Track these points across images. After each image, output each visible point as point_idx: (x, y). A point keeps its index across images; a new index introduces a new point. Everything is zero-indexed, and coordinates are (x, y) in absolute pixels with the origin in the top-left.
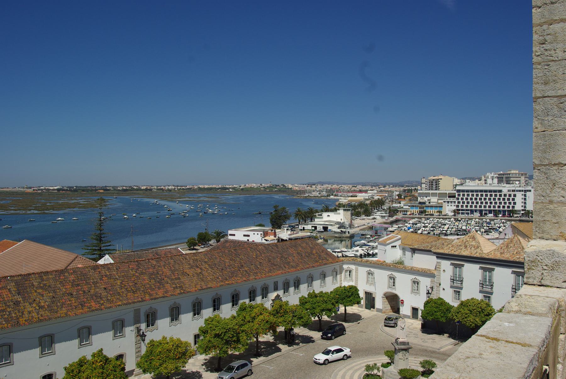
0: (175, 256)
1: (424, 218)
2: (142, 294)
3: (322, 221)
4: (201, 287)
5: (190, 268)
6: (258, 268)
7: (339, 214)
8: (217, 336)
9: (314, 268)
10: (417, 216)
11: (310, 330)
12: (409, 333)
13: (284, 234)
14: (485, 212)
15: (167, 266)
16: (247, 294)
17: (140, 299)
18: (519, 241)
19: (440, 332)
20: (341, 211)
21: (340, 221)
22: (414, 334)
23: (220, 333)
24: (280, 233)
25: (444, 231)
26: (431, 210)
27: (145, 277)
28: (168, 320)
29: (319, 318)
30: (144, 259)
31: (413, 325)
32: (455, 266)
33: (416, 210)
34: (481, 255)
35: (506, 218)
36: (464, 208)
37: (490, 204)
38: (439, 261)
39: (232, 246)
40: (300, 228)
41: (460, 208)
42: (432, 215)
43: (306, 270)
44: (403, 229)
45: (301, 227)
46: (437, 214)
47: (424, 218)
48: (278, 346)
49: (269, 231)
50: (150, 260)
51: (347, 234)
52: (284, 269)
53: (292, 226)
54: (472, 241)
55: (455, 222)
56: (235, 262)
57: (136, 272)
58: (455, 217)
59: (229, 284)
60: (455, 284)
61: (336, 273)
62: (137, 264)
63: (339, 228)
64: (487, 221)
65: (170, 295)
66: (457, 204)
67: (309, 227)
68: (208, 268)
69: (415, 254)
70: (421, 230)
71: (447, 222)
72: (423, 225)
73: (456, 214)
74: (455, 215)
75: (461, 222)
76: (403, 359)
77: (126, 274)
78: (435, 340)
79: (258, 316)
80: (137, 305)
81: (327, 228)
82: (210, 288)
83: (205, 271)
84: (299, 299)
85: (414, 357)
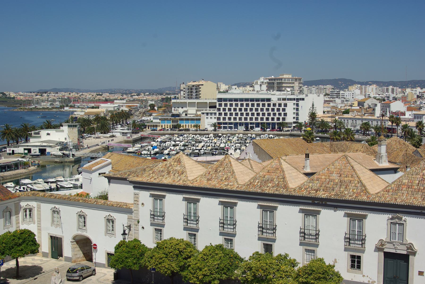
10: (169, 132)
31: (106, 276)
32: (155, 197)
34: (185, 183)
38: (137, 191)
42: (188, 130)
54: (177, 165)
60: (155, 220)
69: (111, 184)
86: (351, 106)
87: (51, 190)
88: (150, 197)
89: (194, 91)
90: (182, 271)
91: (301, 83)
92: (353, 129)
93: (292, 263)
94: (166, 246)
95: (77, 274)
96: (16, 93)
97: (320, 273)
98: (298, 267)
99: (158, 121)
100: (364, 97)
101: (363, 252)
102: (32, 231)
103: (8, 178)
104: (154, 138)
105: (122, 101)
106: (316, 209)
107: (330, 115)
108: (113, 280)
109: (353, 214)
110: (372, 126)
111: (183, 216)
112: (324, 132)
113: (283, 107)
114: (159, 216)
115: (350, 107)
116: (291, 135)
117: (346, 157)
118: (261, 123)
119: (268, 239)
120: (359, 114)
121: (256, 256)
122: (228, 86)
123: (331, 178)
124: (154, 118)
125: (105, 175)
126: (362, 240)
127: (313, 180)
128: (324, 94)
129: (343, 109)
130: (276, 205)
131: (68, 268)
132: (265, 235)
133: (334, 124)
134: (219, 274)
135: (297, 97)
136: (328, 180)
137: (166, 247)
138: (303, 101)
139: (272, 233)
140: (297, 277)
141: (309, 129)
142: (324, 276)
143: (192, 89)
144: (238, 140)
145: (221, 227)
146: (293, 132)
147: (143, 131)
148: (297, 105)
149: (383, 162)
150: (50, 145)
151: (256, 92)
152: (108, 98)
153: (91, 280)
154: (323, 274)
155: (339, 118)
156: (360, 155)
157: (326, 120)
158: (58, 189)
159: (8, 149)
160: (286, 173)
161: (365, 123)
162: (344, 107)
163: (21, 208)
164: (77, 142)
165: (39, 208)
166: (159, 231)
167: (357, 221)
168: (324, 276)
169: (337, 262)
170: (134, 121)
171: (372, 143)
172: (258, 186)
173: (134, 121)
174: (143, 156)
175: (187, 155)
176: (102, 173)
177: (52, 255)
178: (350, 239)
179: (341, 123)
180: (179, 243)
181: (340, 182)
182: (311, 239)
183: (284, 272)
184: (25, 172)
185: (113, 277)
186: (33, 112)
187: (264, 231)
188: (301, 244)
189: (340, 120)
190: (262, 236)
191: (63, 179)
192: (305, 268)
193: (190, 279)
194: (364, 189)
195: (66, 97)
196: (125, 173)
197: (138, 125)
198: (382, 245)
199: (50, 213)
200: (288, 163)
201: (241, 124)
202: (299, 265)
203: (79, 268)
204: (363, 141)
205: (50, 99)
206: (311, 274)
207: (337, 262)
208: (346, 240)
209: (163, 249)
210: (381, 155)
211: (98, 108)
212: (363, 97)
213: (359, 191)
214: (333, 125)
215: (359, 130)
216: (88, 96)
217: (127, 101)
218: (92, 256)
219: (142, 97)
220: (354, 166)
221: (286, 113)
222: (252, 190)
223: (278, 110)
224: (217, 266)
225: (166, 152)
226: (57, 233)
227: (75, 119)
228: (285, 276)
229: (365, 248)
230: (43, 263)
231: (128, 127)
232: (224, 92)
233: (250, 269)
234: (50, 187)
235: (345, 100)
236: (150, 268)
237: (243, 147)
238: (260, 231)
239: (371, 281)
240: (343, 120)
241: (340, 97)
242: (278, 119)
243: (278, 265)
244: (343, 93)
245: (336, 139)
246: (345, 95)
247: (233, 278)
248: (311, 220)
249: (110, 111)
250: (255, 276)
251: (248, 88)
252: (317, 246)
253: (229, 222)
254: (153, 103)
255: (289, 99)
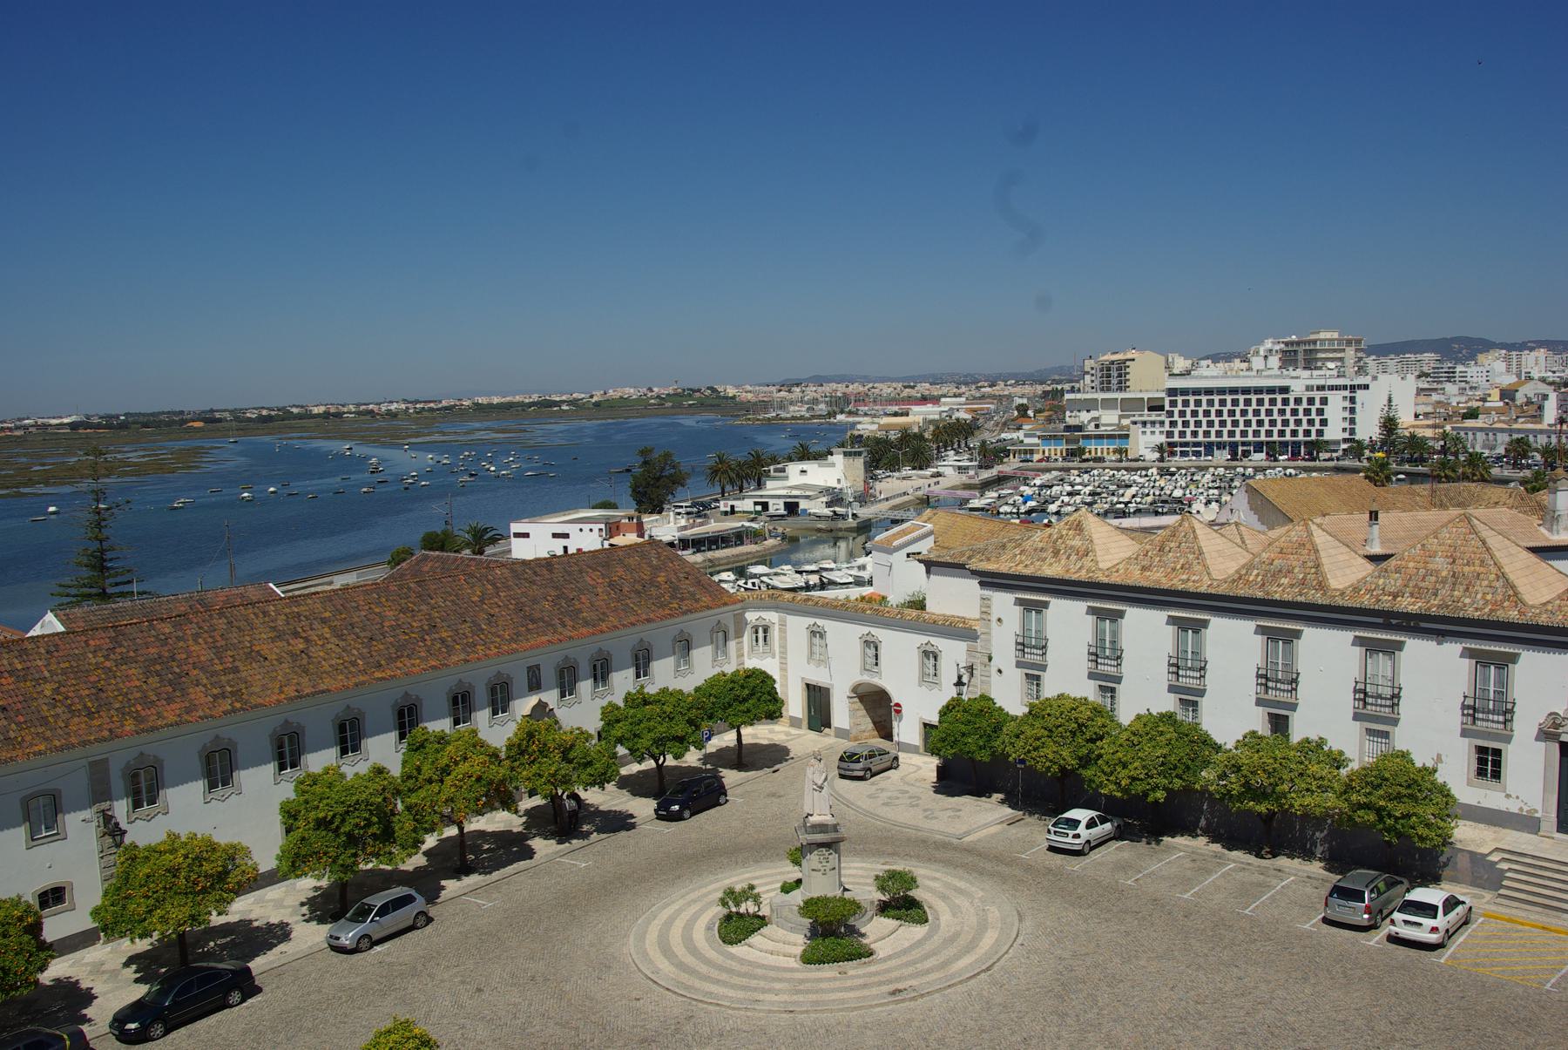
0: (235, 606)
1: (1079, 469)
2: (115, 719)
3: (784, 488)
4: (297, 691)
5: (273, 640)
6: (483, 630)
7: (833, 465)
8: (322, 824)
9: (653, 625)
11: (635, 795)
12: (900, 795)
13: (667, 527)
14: (1245, 448)
15: (205, 635)
16: (445, 704)
17: (106, 733)
18: (1194, 532)
19: (981, 791)
20: (838, 458)
21: (835, 485)
22: (910, 798)
23: (329, 817)
24: (655, 524)
25: (1120, 503)
26: (1099, 448)
27: (130, 672)
28: (199, 786)
29: (657, 761)
30: (135, 621)
32: (1028, 606)
33: (1057, 450)
34: (1091, 574)
35: (1300, 463)
36: (1189, 438)
37: (1258, 426)
38: (987, 593)
39: (438, 570)
40: (723, 509)
41: (1176, 438)
42: (1101, 460)
43: (623, 632)
44: (1011, 501)
45: (726, 506)
46: (1114, 458)
47: (1079, 469)
48: (530, 842)
49: (623, 521)
50: (155, 622)
51: (850, 520)
52: (560, 629)
53: (702, 504)
55: (1158, 477)
56: (414, 616)
57: (107, 657)
58: (1161, 464)
59: (383, 679)
61: (722, 636)
62: (114, 635)
63: (828, 505)
64: (1247, 474)
65: (200, 717)
66: (1167, 427)
67: (746, 505)
68: (328, 636)
70: (1058, 503)
71: (1136, 478)
72: (1069, 488)
73: (1166, 455)
74: (1161, 459)
75: (1174, 478)
76: (822, 871)
77: (75, 665)
78: (960, 810)
79: (456, 763)
80: (97, 751)
81: (797, 504)
82: (323, 692)
83: (316, 645)
84: (600, 712)
85: (882, 861)
86: (1484, 400)
87: (808, 588)
88: (1015, 604)
89: (1115, 373)
90: (1084, 767)
91: (1362, 350)
92: (1487, 453)
93: (1335, 759)
94: (1048, 711)
95: (860, 766)
96: (737, 387)
97: (1401, 786)
98: (1348, 769)
99: (1035, 440)
100: (1516, 380)
101: (1508, 739)
102: (770, 672)
103: (721, 562)
104: (1026, 479)
105: (958, 400)
106: (1394, 638)
107: (1430, 422)
108: (935, 780)
109: (1482, 650)
110: (1534, 445)
111: (1087, 648)
112: (1416, 461)
113: (1317, 405)
114: (1035, 647)
115: (1480, 404)
116: (1338, 470)
117: (1468, 518)
118: (1268, 443)
119: (1278, 704)
120: (1502, 418)
121: (1252, 740)
122: (1190, 362)
123: (1430, 566)
124: (1026, 436)
125: (920, 557)
126: (1505, 713)
127: (1386, 571)
128: (1417, 373)
129: (1464, 408)
130: (1298, 628)
131: (842, 752)
132: (1272, 695)
133: (1442, 443)
134: (1165, 777)
135: (1353, 383)
136: (1422, 572)
137: (1049, 715)
138: (1366, 391)
139: (1288, 691)
140: (1345, 792)
141: (1380, 454)
142: (1410, 791)
143: (1109, 369)
144: (1213, 482)
145: (1173, 673)
146: (1341, 463)
147: (1002, 463)
148: (1353, 400)
149: (1561, 531)
150: (808, 493)
151: (1254, 373)
152: (927, 393)
153: (889, 778)
154: (1409, 787)
155: (1453, 429)
156: (1503, 514)
157: (1421, 433)
158: (823, 586)
159: (722, 503)
160: (1322, 554)
161: (1518, 441)
162: (1466, 402)
163: (746, 624)
164: (862, 489)
165: (783, 624)
166: (1034, 680)
167: (1492, 667)
168: (1410, 791)
169: (1442, 762)
170: (984, 442)
171: (1535, 485)
172: (1256, 584)
173: (984, 442)
174: (1001, 516)
175: (1098, 514)
176: (914, 554)
177: (809, 723)
178: (1474, 709)
179: (1457, 440)
180: (1078, 707)
181: (1453, 576)
182: (1381, 706)
183: (1315, 779)
184: (757, 551)
185: (935, 774)
186: (773, 426)
187: (1270, 684)
188: (1356, 717)
189: (1455, 433)
190: (1266, 697)
191: (833, 566)
192: (1365, 771)
193: (1101, 785)
194: (1511, 592)
195: (839, 394)
196: (962, 554)
197: (991, 450)
198: (1557, 726)
199: (805, 635)
200: (1327, 532)
201: (1221, 446)
202: (1351, 765)
203: (864, 754)
204: (1512, 481)
205: (806, 399)
206: (1380, 786)
207: (1442, 762)
208: (1466, 712)
209: (1043, 718)
210: (1557, 514)
211: (907, 415)
212: (1512, 379)
213: (1499, 598)
214: (1438, 445)
215: (1505, 456)
216: (886, 389)
217: (967, 399)
218: (891, 728)
219: (1000, 389)
220: (1487, 540)
221: (1326, 420)
222: (1242, 591)
223: (1307, 412)
224: (1161, 759)
225: (1053, 508)
226: (819, 677)
227: (858, 439)
228: (1319, 787)
229: (1512, 730)
230: (792, 740)
231: (971, 454)
232: (1181, 375)
233: (1237, 768)
234: (807, 583)
235: (1467, 386)
236: (1015, 759)
237: (1226, 498)
238: (1261, 684)
239: (1526, 808)
240: (1462, 434)
241: (1457, 379)
242: (1307, 433)
243: (1302, 763)
244: (1464, 369)
245: (1446, 476)
246: (1469, 375)
247: (1197, 787)
248: (1382, 663)
249: (931, 422)
250: (1247, 785)
251: (1237, 364)
252: (1395, 722)
253: (1189, 662)
254: (1025, 401)
255: (1332, 388)
